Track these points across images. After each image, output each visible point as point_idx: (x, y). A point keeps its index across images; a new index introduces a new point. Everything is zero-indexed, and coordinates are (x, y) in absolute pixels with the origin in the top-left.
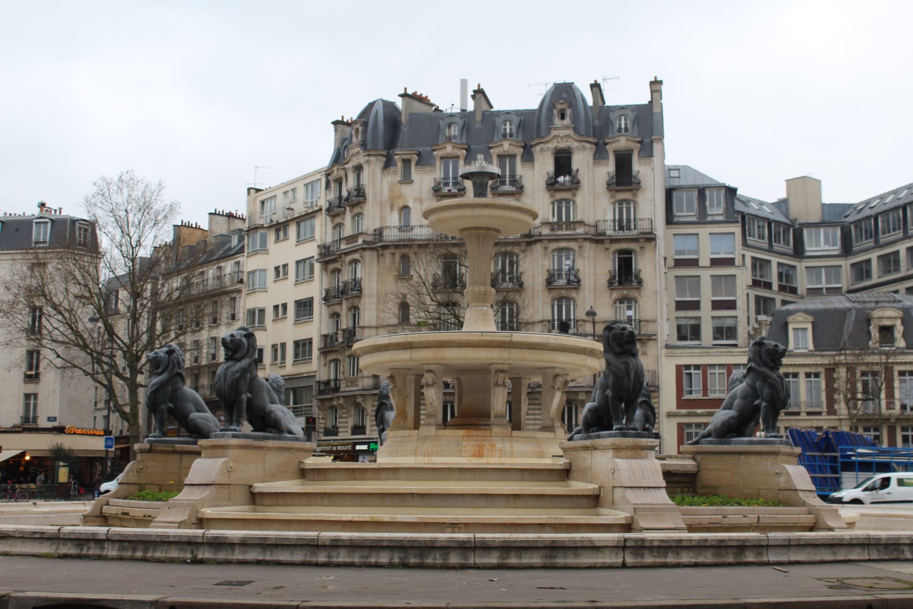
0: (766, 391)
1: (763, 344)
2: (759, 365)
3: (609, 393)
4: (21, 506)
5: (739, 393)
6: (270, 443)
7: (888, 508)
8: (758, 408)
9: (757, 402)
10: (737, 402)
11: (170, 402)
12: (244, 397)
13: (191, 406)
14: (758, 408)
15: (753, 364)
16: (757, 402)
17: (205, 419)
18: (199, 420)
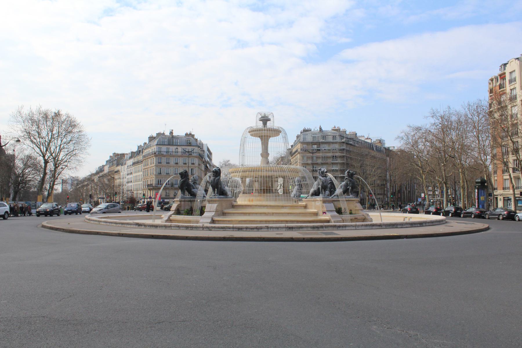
0: (351, 185)
1: (350, 172)
2: (349, 178)
3: (320, 187)
4: (108, 214)
5: (343, 185)
6: (224, 199)
7: (422, 218)
8: (348, 189)
9: (348, 187)
10: (343, 187)
11: (186, 186)
12: (219, 187)
13: (192, 187)
14: (348, 189)
15: (347, 177)
16: (348, 187)
17: (195, 191)
18: (195, 192)
